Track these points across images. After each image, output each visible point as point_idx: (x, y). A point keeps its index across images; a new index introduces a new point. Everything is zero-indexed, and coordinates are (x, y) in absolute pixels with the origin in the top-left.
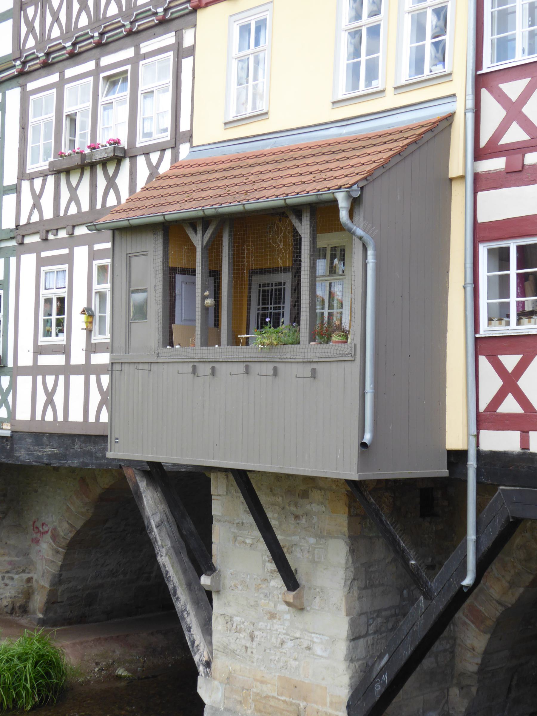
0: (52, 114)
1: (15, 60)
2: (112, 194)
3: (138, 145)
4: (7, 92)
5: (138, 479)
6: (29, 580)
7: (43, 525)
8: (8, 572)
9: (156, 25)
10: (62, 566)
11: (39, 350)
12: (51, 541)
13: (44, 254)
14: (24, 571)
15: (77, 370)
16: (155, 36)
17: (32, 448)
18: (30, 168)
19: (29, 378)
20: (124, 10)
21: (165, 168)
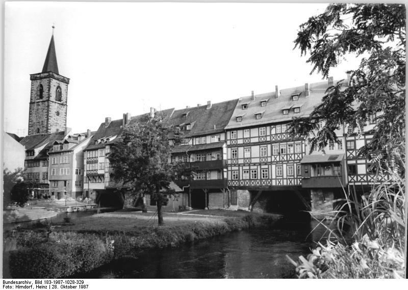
11: (276, 176)
18: (273, 154)
21: (300, 156)
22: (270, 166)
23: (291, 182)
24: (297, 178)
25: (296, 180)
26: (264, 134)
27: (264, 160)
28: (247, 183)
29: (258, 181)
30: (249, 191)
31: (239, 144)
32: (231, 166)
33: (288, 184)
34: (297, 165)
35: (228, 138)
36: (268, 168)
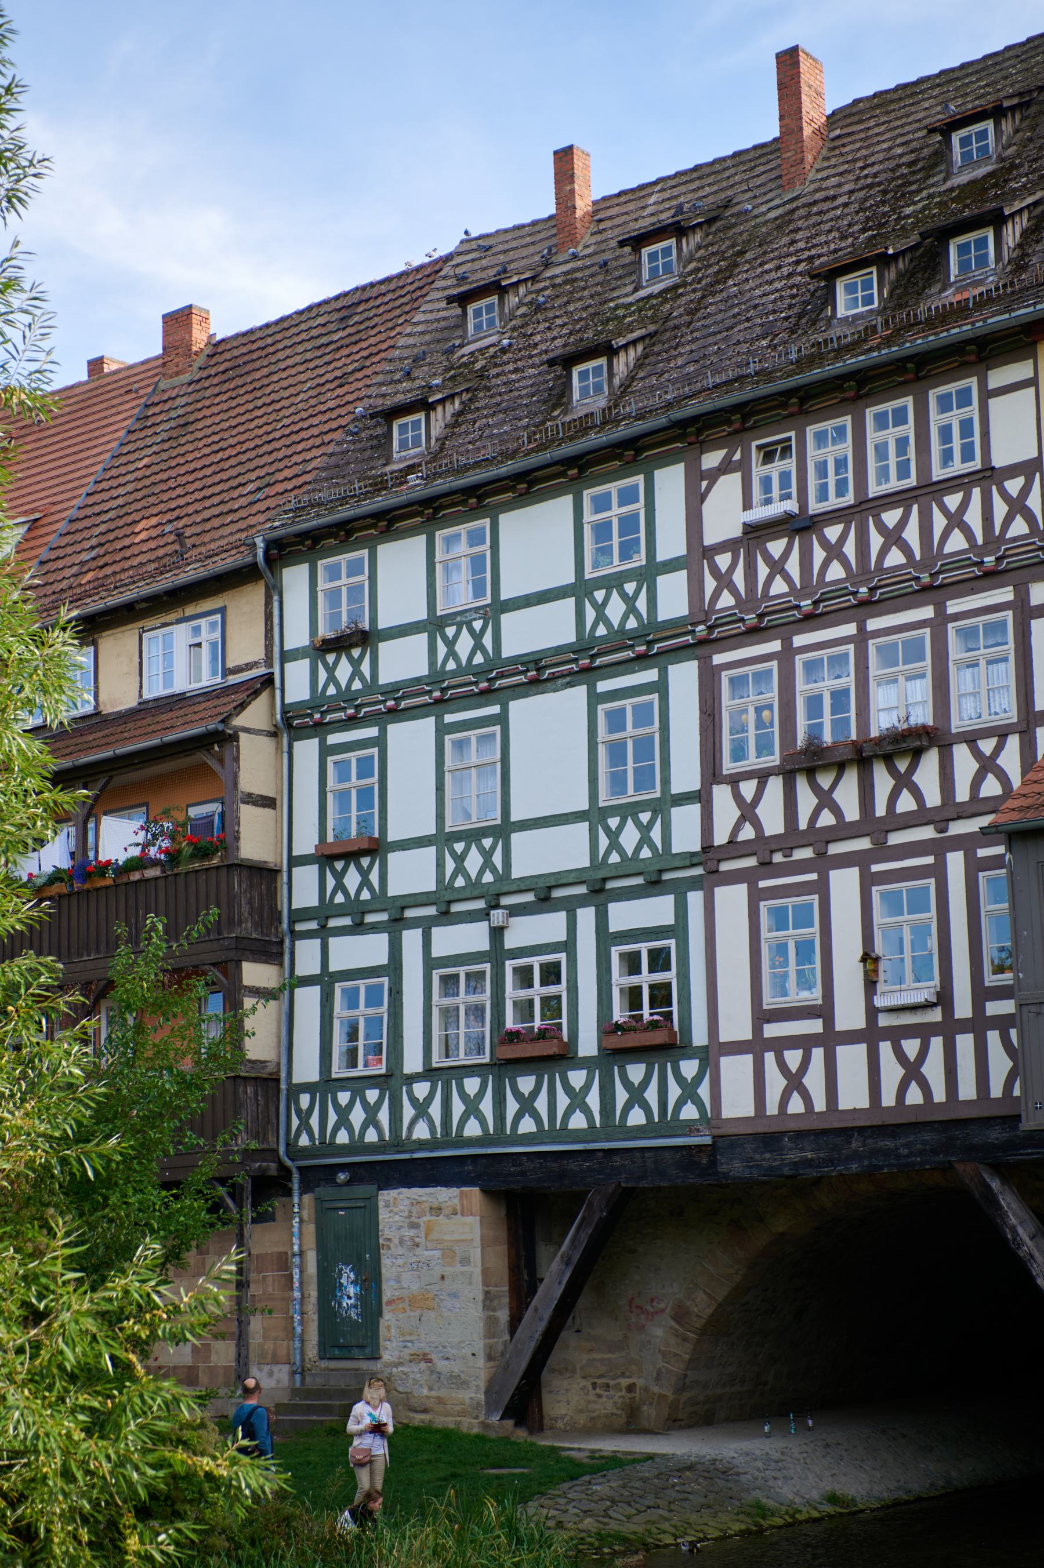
0: (773, 695)
1: (695, 624)
2: (906, 796)
3: (954, 731)
4: (671, 668)
5: (986, 1176)
6: (631, 1388)
7: (652, 1300)
8: (601, 1376)
9: (978, 578)
10: (690, 1361)
11: (761, 1016)
12: (673, 1323)
13: (762, 884)
14: (623, 1375)
15: (851, 1037)
16: (973, 591)
17: (758, 1157)
18: (729, 767)
19: (748, 1059)
20: (918, 557)
21: (1010, 760)
22: (695, 899)
23: (913, 1072)
24: (979, 1025)
25: (965, 1043)
26: (627, 551)
27: (630, 837)
28: (472, 1108)
29: (577, 1078)
30: (486, 1192)
31: (393, 690)
32: (324, 933)
33: (888, 1099)
34: (974, 868)
35: (297, 635)
36: (679, 930)
